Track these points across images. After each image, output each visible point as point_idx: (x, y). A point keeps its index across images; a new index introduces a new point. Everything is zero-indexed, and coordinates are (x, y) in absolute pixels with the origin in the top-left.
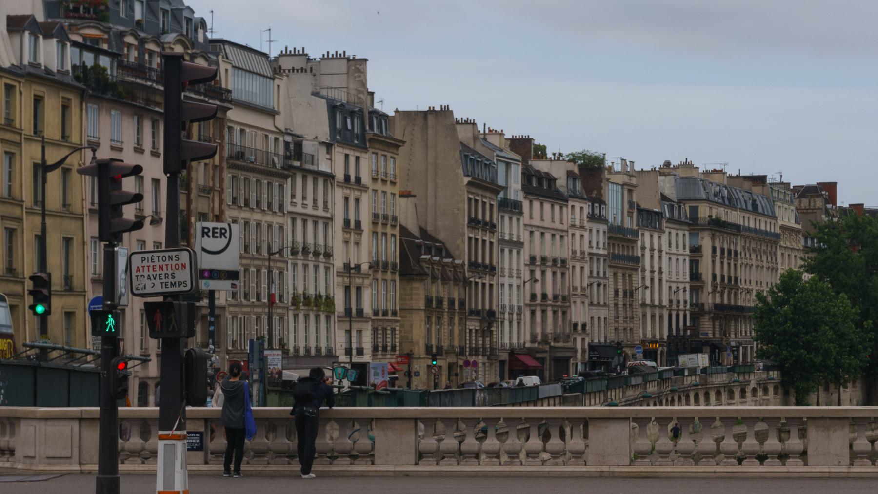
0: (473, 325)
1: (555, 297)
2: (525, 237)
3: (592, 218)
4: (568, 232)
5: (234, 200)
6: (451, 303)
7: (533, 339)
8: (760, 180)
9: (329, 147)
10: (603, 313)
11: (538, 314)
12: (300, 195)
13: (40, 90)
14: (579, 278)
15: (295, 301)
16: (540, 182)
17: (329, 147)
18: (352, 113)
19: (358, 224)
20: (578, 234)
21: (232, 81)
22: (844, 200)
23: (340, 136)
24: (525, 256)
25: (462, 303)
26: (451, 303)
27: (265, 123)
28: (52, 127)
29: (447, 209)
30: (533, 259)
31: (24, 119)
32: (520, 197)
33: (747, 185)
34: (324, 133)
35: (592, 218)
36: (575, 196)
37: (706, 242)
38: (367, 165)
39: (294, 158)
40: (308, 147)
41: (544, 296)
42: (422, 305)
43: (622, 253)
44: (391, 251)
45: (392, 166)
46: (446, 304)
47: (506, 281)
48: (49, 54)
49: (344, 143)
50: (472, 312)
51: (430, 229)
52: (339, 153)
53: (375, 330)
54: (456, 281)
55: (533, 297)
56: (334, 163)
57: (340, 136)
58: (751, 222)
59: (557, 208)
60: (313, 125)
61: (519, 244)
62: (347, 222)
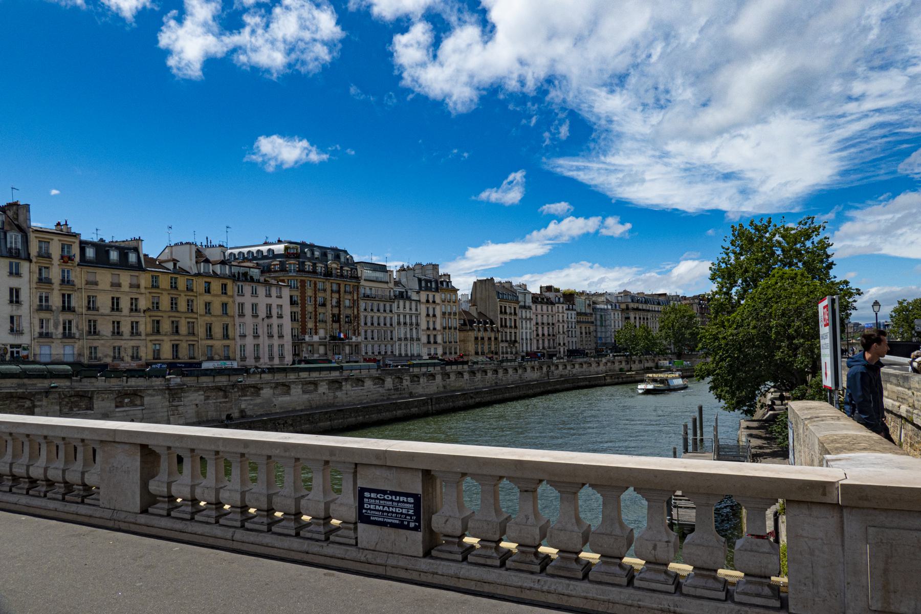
0: (505, 345)
1: (549, 335)
2: (534, 317)
3: (568, 309)
5: (365, 310)
6: (490, 339)
7: (538, 348)
9: (418, 293)
10: (574, 340)
11: (541, 342)
12: (400, 307)
13: (208, 280)
16: (543, 299)
17: (418, 293)
18: (431, 282)
19: (434, 316)
20: (561, 315)
24: (534, 322)
25: (496, 339)
26: (490, 339)
27: (385, 286)
30: (537, 324)
32: (531, 304)
36: (559, 302)
37: (632, 315)
38: (438, 297)
41: (543, 335)
42: (473, 339)
46: (486, 339)
50: (502, 341)
53: (444, 348)
55: (538, 335)
56: (423, 296)
58: (657, 308)
59: (550, 308)
61: (531, 319)
62: (428, 315)
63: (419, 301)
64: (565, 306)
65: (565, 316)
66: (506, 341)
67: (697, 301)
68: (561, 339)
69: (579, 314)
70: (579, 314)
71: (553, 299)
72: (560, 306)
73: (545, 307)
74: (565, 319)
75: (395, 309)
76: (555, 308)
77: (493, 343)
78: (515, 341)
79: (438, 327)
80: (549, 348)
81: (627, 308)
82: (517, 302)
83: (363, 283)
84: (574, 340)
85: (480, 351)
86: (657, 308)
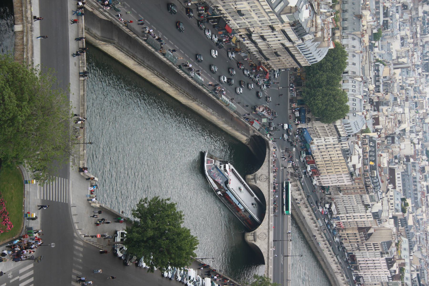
0: (356, 246)
3: (388, 277)
7: (359, 261)
10: (370, 280)
12: (361, 207)
14: (375, 273)
15: (345, 207)
16: (390, 263)
17: (371, 212)
24: (374, 259)
25: (358, 242)
26: (357, 239)
31: (343, 167)
34: (373, 211)
36: (391, 272)
40: (370, 209)
46: (356, 238)
47: (367, 254)
51: (371, 237)
52: (371, 214)
53: (346, 222)
54: (362, 240)
55: (366, 261)
62: (360, 216)
63: (366, 213)
64: (390, 276)
65: (384, 275)
66: (358, 246)
72: (389, 273)
73: (385, 264)
74: (381, 275)
75: (359, 205)
76: (386, 270)
77: (355, 240)
78: (360, 250)
80: (361, 267)
84: (370, 280)
85: (349, 235)
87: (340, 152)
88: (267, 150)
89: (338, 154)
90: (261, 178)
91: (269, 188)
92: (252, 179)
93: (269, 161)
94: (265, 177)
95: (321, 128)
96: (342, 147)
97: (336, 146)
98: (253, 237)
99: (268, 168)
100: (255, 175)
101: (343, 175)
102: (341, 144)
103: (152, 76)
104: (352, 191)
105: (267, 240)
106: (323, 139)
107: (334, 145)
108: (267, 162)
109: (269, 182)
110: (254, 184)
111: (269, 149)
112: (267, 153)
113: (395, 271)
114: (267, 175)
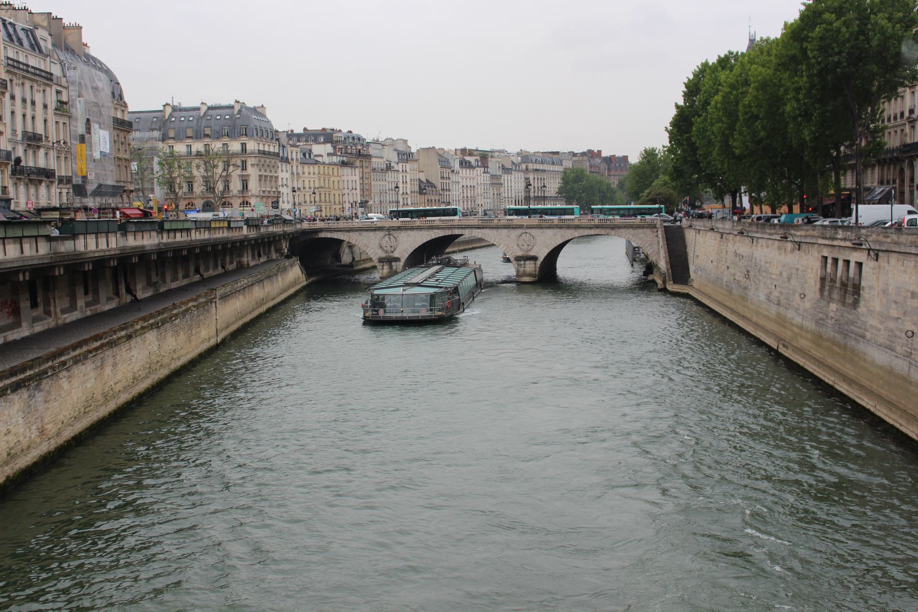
2: (460, 180)
3: (484, 172)
4: (477, 177)
8: (557, 153)
10: (489, 201)
12: (390, 176)
14: (479, 190)
21: (372, 151)
22: (603, 155)
23: (401, 160)
27: (381, 160)
28: (336, 173)
29: (434, 174)
33: (551, 155)
34: (396, 160)
35: (484, 172)
36: (478, 166)
37: (531, 176)
38: (408, 166)
39: (389, 168)
40: (392, 164)
43: (496, 181)
44: (417, 189)
45: (415, 166)
48: (335, 159)
49: (403, 162)
52: (400, 165)
56: (399, 167)
57: (401, 160)
60: (394, 157)
64: (482, 170)
67: (585, 158)
68: (480, 201)
69: (493, 177)
70: (493, 177)
71: (473, 163)
72: (479, 169)
76: (475, 171)
79: (409, 192)
81: (527, 169)
82: (450, 168)
83: (373, 160)
86: (551, 168)
87: (306, 167)
88: (323, 235)
89: (309, 173)
90: (389, 248)
91: (412, 229)
92: (391, 267)
93: (349, 230)
94: (387, 238)
95: (263, 181)
96: (297, 160)
97: (295, 171)
98: (528, 262)
99: (364, 233)
100: (381, 260)
101: (345, 178)
102: (292, 159)
103: (108, 370)
104: (366, 182)
105: (534, 232)
106: (280, 189)
107: (293, 173)
108: (351, 234)
109: (399, 228)
110: (402, 264)
111: (321, 230)
112: (329, 235)
113: (476, 160)
114: (380, 234)
